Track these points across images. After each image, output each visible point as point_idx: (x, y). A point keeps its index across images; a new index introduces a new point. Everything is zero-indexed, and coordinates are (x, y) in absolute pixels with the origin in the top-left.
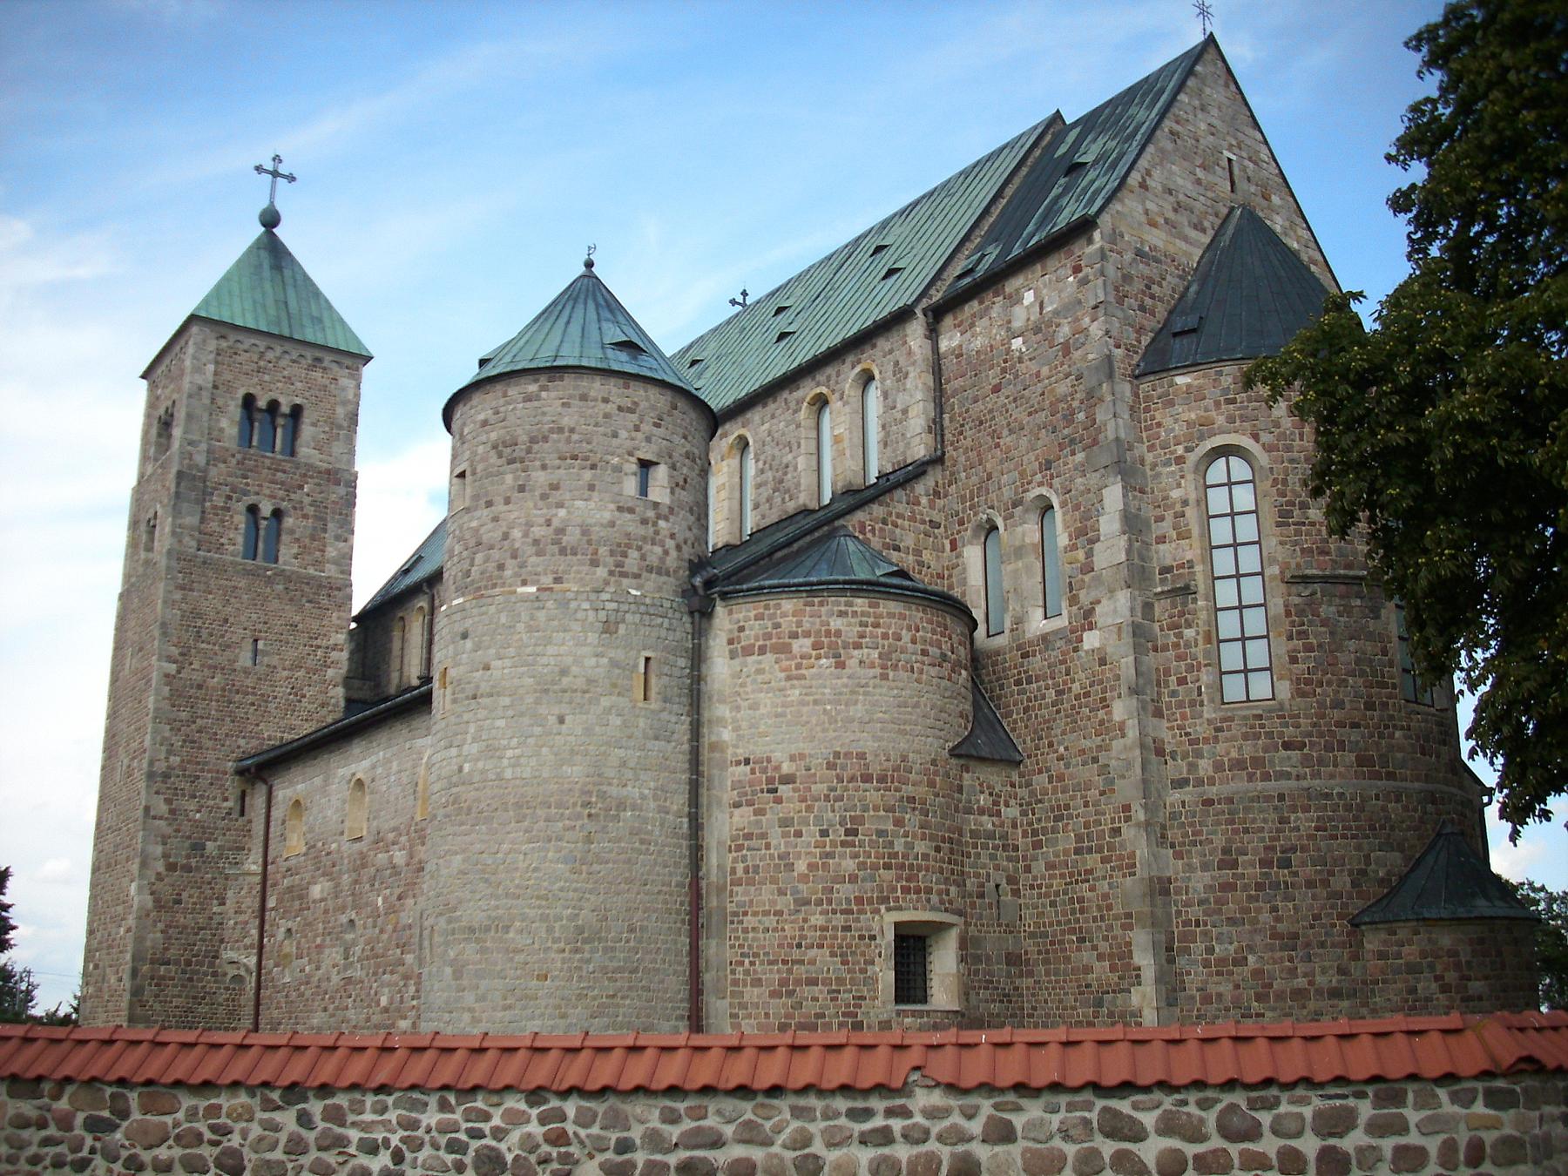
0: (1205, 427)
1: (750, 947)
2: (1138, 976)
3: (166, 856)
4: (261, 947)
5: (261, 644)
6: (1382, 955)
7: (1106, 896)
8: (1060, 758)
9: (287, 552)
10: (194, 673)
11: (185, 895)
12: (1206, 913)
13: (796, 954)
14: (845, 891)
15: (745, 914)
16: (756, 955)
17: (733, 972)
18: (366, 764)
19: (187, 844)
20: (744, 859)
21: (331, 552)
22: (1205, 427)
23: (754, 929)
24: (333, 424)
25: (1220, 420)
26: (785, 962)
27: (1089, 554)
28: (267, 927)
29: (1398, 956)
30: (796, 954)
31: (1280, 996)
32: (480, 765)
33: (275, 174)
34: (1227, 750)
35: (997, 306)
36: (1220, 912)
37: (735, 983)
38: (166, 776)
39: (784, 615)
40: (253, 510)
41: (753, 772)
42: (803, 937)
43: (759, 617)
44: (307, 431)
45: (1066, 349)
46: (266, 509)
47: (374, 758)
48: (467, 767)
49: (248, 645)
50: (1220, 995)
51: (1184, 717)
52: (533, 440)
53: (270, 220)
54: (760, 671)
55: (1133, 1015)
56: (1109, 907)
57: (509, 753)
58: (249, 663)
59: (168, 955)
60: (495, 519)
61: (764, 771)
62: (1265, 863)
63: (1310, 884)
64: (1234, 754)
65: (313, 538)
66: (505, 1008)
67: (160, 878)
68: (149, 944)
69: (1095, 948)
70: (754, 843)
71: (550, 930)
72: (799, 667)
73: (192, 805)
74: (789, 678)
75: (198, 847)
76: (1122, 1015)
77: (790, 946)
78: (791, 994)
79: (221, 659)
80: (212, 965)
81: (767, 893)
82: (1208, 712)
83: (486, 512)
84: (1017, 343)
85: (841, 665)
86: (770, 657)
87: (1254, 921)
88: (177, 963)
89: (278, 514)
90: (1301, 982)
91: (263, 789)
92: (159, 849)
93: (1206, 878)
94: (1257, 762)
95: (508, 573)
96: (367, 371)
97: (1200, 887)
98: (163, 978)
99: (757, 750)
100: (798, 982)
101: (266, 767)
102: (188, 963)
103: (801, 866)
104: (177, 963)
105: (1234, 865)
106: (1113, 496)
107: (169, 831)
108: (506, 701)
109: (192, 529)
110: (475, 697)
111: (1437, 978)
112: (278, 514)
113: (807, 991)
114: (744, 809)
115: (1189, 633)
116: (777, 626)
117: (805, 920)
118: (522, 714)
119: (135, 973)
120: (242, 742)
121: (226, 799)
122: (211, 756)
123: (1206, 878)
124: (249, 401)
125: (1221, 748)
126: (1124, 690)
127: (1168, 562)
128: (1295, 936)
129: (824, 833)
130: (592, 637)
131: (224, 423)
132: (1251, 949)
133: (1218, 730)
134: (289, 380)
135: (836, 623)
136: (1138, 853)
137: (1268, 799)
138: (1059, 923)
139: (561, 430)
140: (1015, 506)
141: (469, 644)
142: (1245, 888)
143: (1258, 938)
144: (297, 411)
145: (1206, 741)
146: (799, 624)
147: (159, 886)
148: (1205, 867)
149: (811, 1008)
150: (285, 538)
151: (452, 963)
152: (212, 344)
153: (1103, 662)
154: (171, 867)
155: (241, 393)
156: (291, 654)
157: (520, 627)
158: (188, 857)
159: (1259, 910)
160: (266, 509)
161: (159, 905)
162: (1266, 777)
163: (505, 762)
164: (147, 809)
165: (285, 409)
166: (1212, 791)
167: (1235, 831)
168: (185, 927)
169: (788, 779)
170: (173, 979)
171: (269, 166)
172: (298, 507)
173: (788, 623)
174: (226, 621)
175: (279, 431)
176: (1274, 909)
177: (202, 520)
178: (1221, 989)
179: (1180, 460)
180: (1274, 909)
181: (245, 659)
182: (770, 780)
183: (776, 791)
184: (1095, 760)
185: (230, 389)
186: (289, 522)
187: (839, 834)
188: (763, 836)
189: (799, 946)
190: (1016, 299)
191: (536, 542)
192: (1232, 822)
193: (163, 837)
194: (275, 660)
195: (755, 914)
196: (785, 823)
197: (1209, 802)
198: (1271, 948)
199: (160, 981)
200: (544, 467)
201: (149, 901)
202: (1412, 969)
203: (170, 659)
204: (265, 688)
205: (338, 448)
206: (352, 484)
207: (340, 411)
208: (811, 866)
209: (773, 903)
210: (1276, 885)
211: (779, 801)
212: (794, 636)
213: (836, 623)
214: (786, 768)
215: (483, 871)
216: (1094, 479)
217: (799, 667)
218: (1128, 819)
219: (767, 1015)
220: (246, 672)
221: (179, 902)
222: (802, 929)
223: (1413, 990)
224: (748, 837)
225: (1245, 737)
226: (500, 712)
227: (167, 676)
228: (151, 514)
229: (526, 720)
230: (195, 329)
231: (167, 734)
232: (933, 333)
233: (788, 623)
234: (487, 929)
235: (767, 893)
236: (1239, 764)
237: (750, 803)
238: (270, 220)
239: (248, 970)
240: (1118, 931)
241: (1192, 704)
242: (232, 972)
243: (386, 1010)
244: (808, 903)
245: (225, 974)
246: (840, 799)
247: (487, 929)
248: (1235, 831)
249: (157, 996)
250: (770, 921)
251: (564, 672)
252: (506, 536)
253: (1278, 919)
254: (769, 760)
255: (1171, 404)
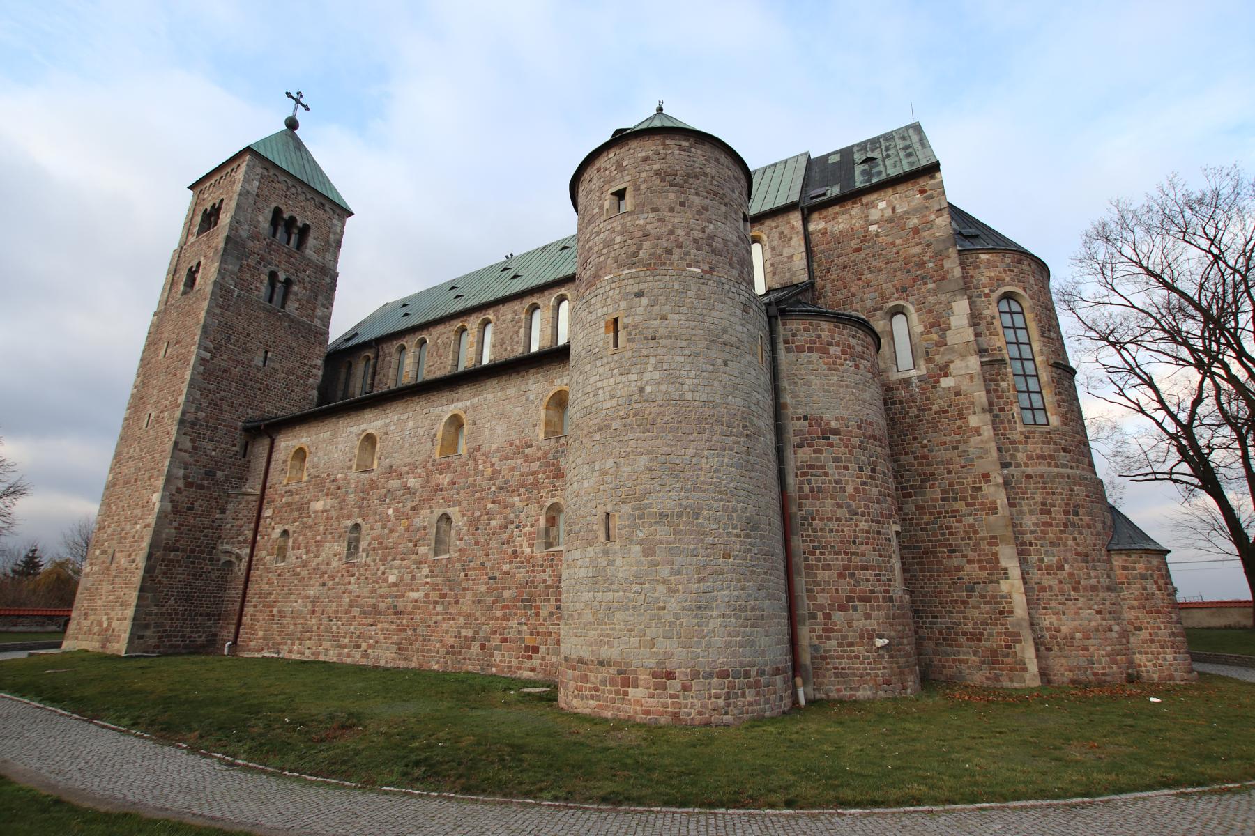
0: (1000, 282)
1: (819, 542)
2: (1006, 574)
3: (185, 477)
4: (254, 542)
5: (269, 355)
6: (1125, 568)
7: (971, 526)
8: (925, 446)
9: (292, 306)
10: (222, 361)
11: (196, 505)
12: (1036, 538)
13: (853, 548)
14: (875, 508)
15: (814, 519)
16: (824, 547)
17: (806, 559)
18: (379, 423)
19: (203, 471)
20: (809, 482)
21: (319, 313)
22: (1000, 282)
23: (821, 530)
24: (327, 243)
25: (1007, 279)
26: (846, 553)
27: (943, 336)
28: (261, 529)
29: (1134, 569)
30: (853, 548)
31: (1085, 589)
32: (663, 388)
33: (298, 102)
34: (1036, 448)
35: (856, 209)
36: (1044, 538)
37: (809, 567)
38: (193, 424)
39: (823, 330)
40: (273, 276)
41: (810, 425)
42: (856, 537)
43: (805, 329)
44: (311, 241)
45: (916, 231)
46: (282, 276)
47: (388, 420)
48: (648, 389)
49: (261, 353)
50: (1050, 587)
51: (1005, 429)
52: (688, 176)
53: (292, 124)
54: (810, 363)
55: (1003, 597)
56: (976, 532)
57: (689, 381)
58: (261, 364)
59: (178, 544)
60: (662, 220)
61: (819, 425)
62: (1066, 512)
63: (1089, 526)
64: (1038, 451)
65: (308, 302)
66: (700, 581)
67: (179, 490)
68: (164, 536)
69: (964, 556)
70: (815, 471)
71: (730, 519)
72: (835, 363)
73: (210, 446)
74: (829, 369)
75: (210, 474)
76: (994, 597)
77: (849, 542)
78: (852, 576)
79: (243, 357)
80: (210, 553)
81: (829, 506)
82: (1019, 427)
83: (651, 215)
84: (873, 228)
85: (857, 367)
86: (815, 355)
87: (1065, 545)
88: (184, 551)
89: (288, 283)
90: (1093, 581)
91: (267, 441)
92: (181, 472)
93: (1034, 518)
94: (1051, 457)
95: (675, 257)
96: (349, 220)
97: (1030, 523)
98: (172, 561)
99: (812, 411)
100: (856, 568)
101: (268, 429)
102: (193, 551)
103: (850, 489)
104: (184, 551)
105: (1049, 512)
106: (961, 307)
107: (191, 460)
108: (684, 344)
109: (232, 273)
110: (653, 338)
111: (1156, 582)
112: (288, 283)
113: (861, 574)
114: (806, 449)
115: (1003, 385)
116: (819, 336)
117: (857, 526)
118: (697, 355)
119: (150, 556)
120: (250, 411)
121: (234, 445)
122: (227, 416)
123: (1034, 518)
124: (277, 212)
125: (1030, 447)
126: (978, 409)
127: (985, 346)
128: (1087, 555)
129: (861, 469)
130: (739, 312)
131: (261, 219)
132: (1066, 560)
133: (1027, 437)
134: (303, 208)
135: (853, 341)
136: (999, 501)
137: (1063, 477)
138: (931, 541)
139: (706, 175)
140: (876, 310)
141: (644, 301)
142: (1057, 525)
143: (1069, 554)
144: (305, 230)
145: (1020, 443)
146: (833, 338)
147: (178, 497)
148: (1031, 512)
149: (865, 586)
150: (292, 297)
151: (641, 543)
152: (259, 170)
153: (958, 394)
154: (189, 485)
155: (274, 205)
156: (288, 365)
157: (691, 294)
158: (203, 479)
159: (1066, 539)
160: (282, 276)
161: (176, 510)
162: (1057, 466)
163: (686, 387)
164: (176, 444)
165: (299, 224)
166: (1030, 470)
167: (1048, 494)
168: (194, 526)
169: (836, 432)
170: (179, 561)
171: (295, 96)
172: (301, 281)
173: (826, 336)
174: (249, 335)
175: (293, 237)
176: (1075, 539)
177: (240, 271)
178: (1051, 583)
179: (987, 296)
180: (1075, 539)
181: (258, 361)
182: (823, 432)
183: (828, 438)
184: (955, 448)
185: (267, 199)
186: (295, 288)
187: (867, 471)
188: (823, 467)
189: (854, 543)
190: (873, 205)
191: (695, 240)
192: (1045, 488)
193: (186, 464)
194: (277, 366)
195: (821, 519)
196: (837, 460)
197: (1029, 476)
198: (1076, 560)
199: (169, 563)
200: (697, 194)
201: (169, 507)
202: (1143, 577)
203: (206, 349)
204: (269, 381)
205: (329, 256)
206: (334, 277)
207: (332, 236)
208: (856, 490)
209: (834, 512)
210: (1073, 525)
211: (831, 445)
212: (830, 344)
213: (853, 341)
214: (834, 424)
215: (673, 469)
216: (943, 298)
217: (835, 363)
218: (988, 482)
219: (837, 590)
220: (258, 369)
221: (191, 509)
222: (855, 531)
223: (1145, 589)
224: (811, 467)
225: (1043, 443)
226: (678, 351)
227: (203, 359)
228: (194, 263)
229: (701, 360)
230: (247, 157)
231: (198, 397)
232: (805, 221)
233: (826, 336)
234: (679, 515)
235: (829, 506)
236: (1041, 457)
237: (810, 445)
238: (292, 124)
239: (239, 558)
240: (984, 546)
241: (1010, 422)
242: (224, 558)
243: (394, 585)
244: (857, 514)
245: (219, 560)
246: (865, 449)
247: (679, 515)
248: (1048, 494)
249: (165, 573)
250: (833, 525)
251: (724, 331)
252: (671, 233)
253: (1078, 544)
254: (822, 419)
255: (979, 267)
